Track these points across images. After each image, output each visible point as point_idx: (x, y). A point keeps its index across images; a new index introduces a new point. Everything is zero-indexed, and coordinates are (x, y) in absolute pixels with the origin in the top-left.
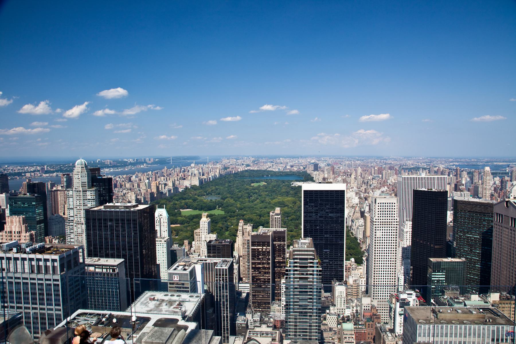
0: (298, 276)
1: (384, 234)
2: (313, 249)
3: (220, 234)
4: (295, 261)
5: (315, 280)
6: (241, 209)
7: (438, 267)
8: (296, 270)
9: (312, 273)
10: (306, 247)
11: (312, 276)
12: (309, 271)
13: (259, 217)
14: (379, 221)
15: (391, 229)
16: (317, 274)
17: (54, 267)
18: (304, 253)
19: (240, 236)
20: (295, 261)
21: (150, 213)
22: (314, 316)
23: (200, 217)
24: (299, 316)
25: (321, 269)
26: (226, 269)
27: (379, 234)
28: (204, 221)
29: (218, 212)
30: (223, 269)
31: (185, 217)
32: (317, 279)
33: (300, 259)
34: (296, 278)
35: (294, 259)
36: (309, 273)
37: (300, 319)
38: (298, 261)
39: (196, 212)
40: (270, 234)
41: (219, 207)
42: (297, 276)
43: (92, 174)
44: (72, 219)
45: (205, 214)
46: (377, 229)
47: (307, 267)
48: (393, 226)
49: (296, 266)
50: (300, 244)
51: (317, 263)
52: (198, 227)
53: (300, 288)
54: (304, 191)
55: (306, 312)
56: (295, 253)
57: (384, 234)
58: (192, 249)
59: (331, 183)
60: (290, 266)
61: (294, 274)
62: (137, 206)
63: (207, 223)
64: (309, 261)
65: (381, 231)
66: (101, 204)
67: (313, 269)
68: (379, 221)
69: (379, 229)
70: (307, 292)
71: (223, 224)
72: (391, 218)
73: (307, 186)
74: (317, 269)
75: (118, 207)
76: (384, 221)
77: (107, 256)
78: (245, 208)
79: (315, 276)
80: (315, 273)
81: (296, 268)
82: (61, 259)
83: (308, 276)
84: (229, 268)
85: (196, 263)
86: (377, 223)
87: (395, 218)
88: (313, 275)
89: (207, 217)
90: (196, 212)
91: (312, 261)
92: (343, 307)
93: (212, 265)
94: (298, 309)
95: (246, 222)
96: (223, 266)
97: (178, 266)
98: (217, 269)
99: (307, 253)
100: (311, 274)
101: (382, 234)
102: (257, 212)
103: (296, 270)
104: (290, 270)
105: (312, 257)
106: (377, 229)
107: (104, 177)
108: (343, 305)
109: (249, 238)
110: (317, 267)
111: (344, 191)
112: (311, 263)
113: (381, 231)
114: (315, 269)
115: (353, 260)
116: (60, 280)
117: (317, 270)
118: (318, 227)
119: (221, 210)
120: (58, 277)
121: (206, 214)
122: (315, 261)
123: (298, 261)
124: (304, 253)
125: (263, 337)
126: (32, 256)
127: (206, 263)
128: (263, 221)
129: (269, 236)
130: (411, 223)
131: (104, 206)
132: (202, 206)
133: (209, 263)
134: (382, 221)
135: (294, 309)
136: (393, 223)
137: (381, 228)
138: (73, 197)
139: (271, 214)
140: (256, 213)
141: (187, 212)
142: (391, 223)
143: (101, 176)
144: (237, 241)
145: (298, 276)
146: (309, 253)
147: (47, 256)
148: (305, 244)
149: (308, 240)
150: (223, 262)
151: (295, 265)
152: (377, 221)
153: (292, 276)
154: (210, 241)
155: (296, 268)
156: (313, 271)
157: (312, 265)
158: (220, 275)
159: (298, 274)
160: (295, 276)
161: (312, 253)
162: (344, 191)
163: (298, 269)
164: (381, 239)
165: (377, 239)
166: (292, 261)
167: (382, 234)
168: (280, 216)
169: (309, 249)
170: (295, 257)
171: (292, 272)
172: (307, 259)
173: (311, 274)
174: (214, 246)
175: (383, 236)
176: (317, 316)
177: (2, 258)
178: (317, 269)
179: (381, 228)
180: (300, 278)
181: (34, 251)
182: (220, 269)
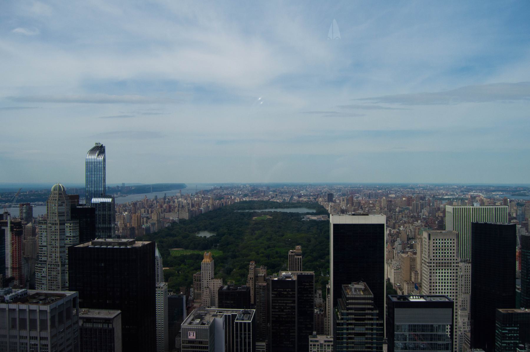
1: (441, 278)
2: (372, 296)
4: (349, 311)
7: (509, 319)
8: (351, 324)
9: (370, 327)
11: (370, 332)
12: (367, 324)
14: (435, 261)
15: (449, 271)
16: (377, 330)
17: (43, 323)
19: (251, 282)
20: (349, 311)
26: (249, 323)
27: (436, 278)
28: (207, 261)
30: (245, 323)
31: (175, 257)
32: (377, 334)
33: (356, 309)
34: (350, 334)
35: (348, 309)
36: (366, 327)
38: (353, 311)
39: (189, 253)
40: (295, 278)
42: (351, 331)
44: (44, 259)
46: (432, 271)
47: (365, 319)
48: (452, 268)
52: (199, 268)
54: (334, 225)
56: (349, 301)
57: (441, 278)
59: (368, 215)
60: (342, 319)
62: (133, 242)
63: (210, 266)
64: (367, 312)
65: (438, 274)
66: (82, 241)
67: (372, 322)
68: (435, 261)
69: (435, 271)
72: (449, 258)
74: (378, 322)
75: (110, 243)
76: (441, 261)
79: (375, 332)
80: (375, 327)
82: (52, 310)
83: (366, 332)
85: (216, 316)
86: (432, 265)
87: (455, 258)
88: (372, 329)
89: (209, 258)
90: (189, 253)
93: (229, 318)
95: (258, 263)
96: (245, 318)
97: (193, 320)
98: (237, 323)
100: (369, 329)
101: (438, 278)
103: (351, 324)
104: (342, 323)
106: (432, 271)
107: (84, 207)
110: (377, 319)
111: (383, 225)
113: (438, 274)
114: (375, 322)
116: (49, 339)
120: (47, 334)
121: (209, 254)
122: (375, 312)
123: (353, 311)
126: (13, 306)
127: (226, 316)
130: (470, 265)
131: (93, 244)
134: (438, 261)
136: (452, 265)
137: (438, 271)
138: (47, 232)
140: (263, 253)
141: (176, 252)
142: (449, 265)
147: (33, 307)
148: (360, 290)
149: (361, 286)
150: (244, 314)
152: (432, 261)
153: (345, 331)
154: (221, 288)
155: (349, 322)
156: (372, 325)
157: (370, 317)
160: (349, 331)
161: (371, 301)
163: (354, 322)
164: (438, 284)
165: (432, 284)
166: (345, 311)
167: (438, 278)
168: (301, 257)
169: (366, 296)
170: (349, 306)
171: (345, 327)
172: (364, 309)
173: (369, 329)
175: (441, 281)
177: (3, 310)
178: (378, 322)
179: (438, 271)
181: (16, 300)
182: (241, 323)
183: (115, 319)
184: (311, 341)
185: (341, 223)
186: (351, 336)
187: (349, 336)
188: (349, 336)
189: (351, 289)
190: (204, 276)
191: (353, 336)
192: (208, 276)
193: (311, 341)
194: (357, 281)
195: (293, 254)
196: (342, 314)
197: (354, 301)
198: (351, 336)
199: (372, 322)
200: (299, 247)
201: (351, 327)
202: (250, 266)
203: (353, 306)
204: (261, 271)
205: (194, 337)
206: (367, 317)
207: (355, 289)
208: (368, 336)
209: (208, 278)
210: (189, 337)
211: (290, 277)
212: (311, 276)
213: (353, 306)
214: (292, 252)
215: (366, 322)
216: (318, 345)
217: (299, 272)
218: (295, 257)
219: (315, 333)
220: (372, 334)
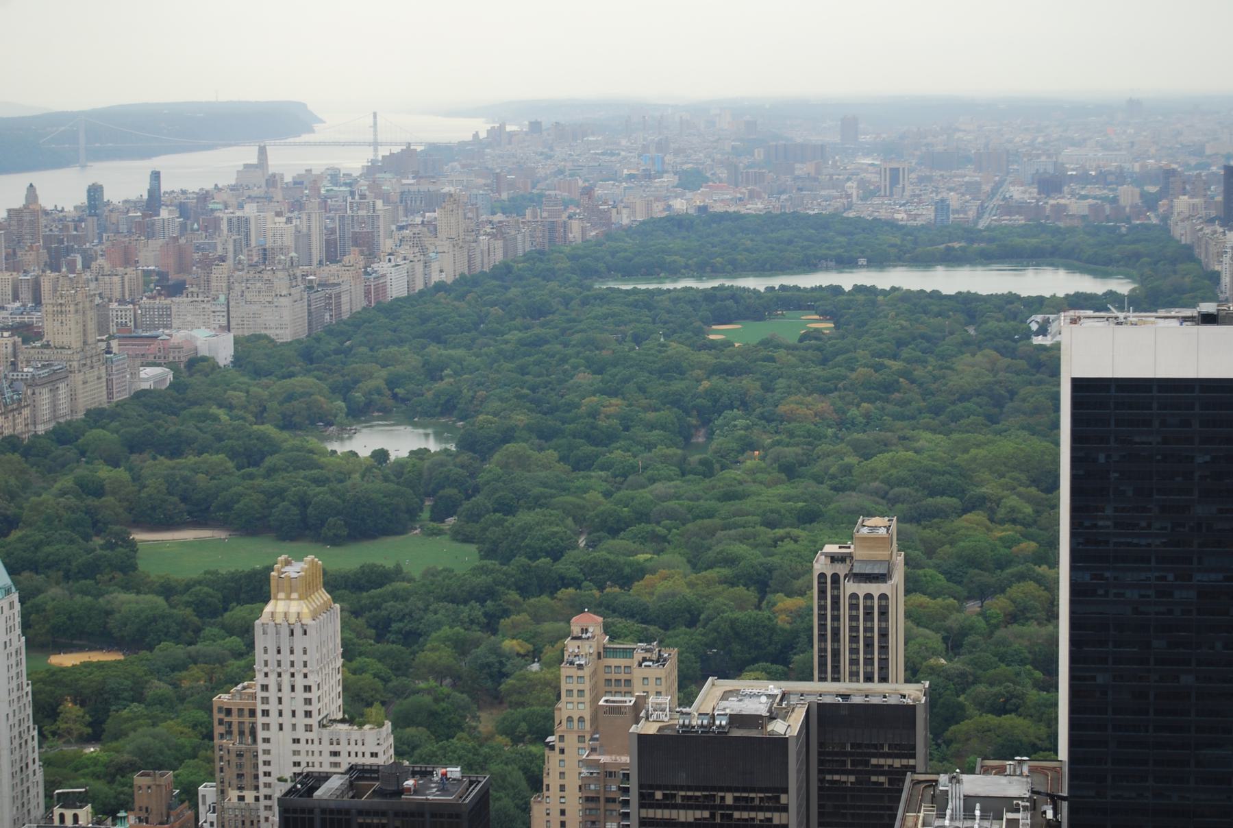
3: (427, 730)
6: (614, 532)
13: (751, 594)
19: (571, 742)
29: (422, 554)
31: (167, 590)
40: (788, 727)
41: (438, 516)
45: (295, 566)
54: (1079, 385)
71: (461, 647)
78: (642, 516)
102: (739, 549)
109: (625, 759)
118: (1187, 680)
128: (782, 621)
129: (782, 742)
132: (303, 503)
139: (821, 565)
140: (730, 561)
141: (179, 551)
144: (551, 780)
154: (310, 782)
185: (1116, 376)
189: (940, 802)
190: (273, 707)
192: (301, 709)
195: (842, 569)
200: (879, 525)
202: (571, 646)
204: (638, 674)
209: (301, 720)
214: (834, 559)
217: (830, 686)
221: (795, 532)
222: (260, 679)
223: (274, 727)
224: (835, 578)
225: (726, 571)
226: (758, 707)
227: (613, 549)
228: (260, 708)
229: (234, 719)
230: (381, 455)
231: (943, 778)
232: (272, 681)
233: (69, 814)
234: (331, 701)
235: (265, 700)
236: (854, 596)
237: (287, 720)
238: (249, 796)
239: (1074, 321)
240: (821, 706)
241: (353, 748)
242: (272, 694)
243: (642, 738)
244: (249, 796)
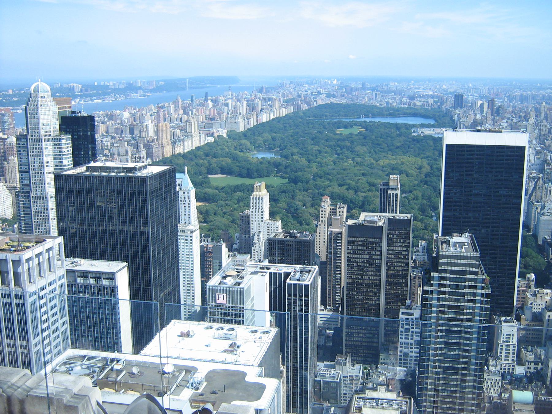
0: (447, 303)
4: (443, 275)
5: (477, 311)
6: (321, 177)
8: (444, 293)
9: (472, 298)
10: (463, 250)
11: (471, 304)
18: (459, 261)
20: (443, 275)
21: (167, 181)
22: (470, 375)
23: (251, 189)
24: (444, 373)
25: (490, 292)
26: (307, 286)
30: (301, 285)
32: (481, 309)
33: (452, 272)
34: (443, 306)
36: (466, 298)
37: (445, 379)
38: (448, 275)
42: (444, 303)
43: (59, 108)
49: (444, 286)
50: (452, 244)
51: (483, 281)
52: (248, 206)
53: (448, 325)
54: (447, 146)
55: (457, 369)
56: (444, 260)
58: (235, 246)
59: (501, 132)
60: (432, 285)
61: (438, 300)
62: (145, 167)
64: (467, 276)
67: (475, 291)
70: (460, 332)
73: (452, 138)
74: (483, 291)
77: (94, 256)
79: (478, 305)
80: (478, 298)
81: (442, 289)
84: (312, 283)
91: (473, 276)
92: (510, 362)
94: (440, 361)
98: (289, 285)
99: (465, 261)
100: (469, 301)
103: (444, 293)
104: (432, 291)
105: (474, 269)
107: (79, 115)
108: (510, 359)
109: (344, 230)
110: (483, 288)
111: (524, 147)
112: (470, 280)
114: (479, 291)
115: (532, 276)
117: (482, 295)
118: (470, 215)
119: (282, 177)
123: (448, 275)
124: (459, 261)
125: (383, 408)
127: (270, 273)
129: (381, 228)
131: (88, 168)
132: (248, 169)
133: (275, 274)
135: (435, 361)
141: (219, 179)
143: (73, 112)
145: (447, 303)
146: (468, 262)
148: (461, 244)
149: (465, 238)
151: (442, 282)
153: (434, 302)
155: (442, 289)
156: (475, 295)
157: (473, 284)
158: (295, 295)
159: (445, 300)
160: (441, 303)
161: (474, 262)
162: (524, 147)
166: (436, 275)
170: (443, 268)
171: (435, 296)
172: (464, 273)
173: (469, 301)
174: (281, 242)
176: (475, 376)
178: (483, 291)
180: (450, 307)
182: (295, 285)
183: (119, 273)
184: (403, 314)
186: (443, 309)
187: (441, 309)
188: (441, 309)
190: (254, 216)
191: (446, 309)
192: (261, 217)
193: (403, 314)
194: (461, 232)
196: (433, 278)
197: (449, 261)
198: (443, 309)
199: (475, 291)
201: (444, 296)
202: (322, 204)
203: (449, 268)
205: (225, 302)
206: (467, 283)
207: (455, 243)
208: (468, 311)
209: (261, 220)
210: (218, 301)
211: (375, 222)
212: (407, 222)
213: (449, 268)
215: (466, 290)
216: (412, 319)
218: (389, 192)
219: (408, 302)
220: (474, 308)
221: (363, 178)
222: (251, 210)
223: (254, 221)
224: (384, 189)
225: (347, 187)
226: (376, 219)
227: (319, 182)
228: (251, 216)
229: (244, 219)
230: (263, 158)
231: (447, 237)
232: (254, 210)
233: (206, 240)
234: (267, 215)
235: (252, 215)
236: (390, 193)
237: (258, 220)
238: (247, 236)
239: (446, 130)
240: (389, 219)
241: (272, 226)
242: (254, 213)
243: (349, 225)
244: (247, 236)
